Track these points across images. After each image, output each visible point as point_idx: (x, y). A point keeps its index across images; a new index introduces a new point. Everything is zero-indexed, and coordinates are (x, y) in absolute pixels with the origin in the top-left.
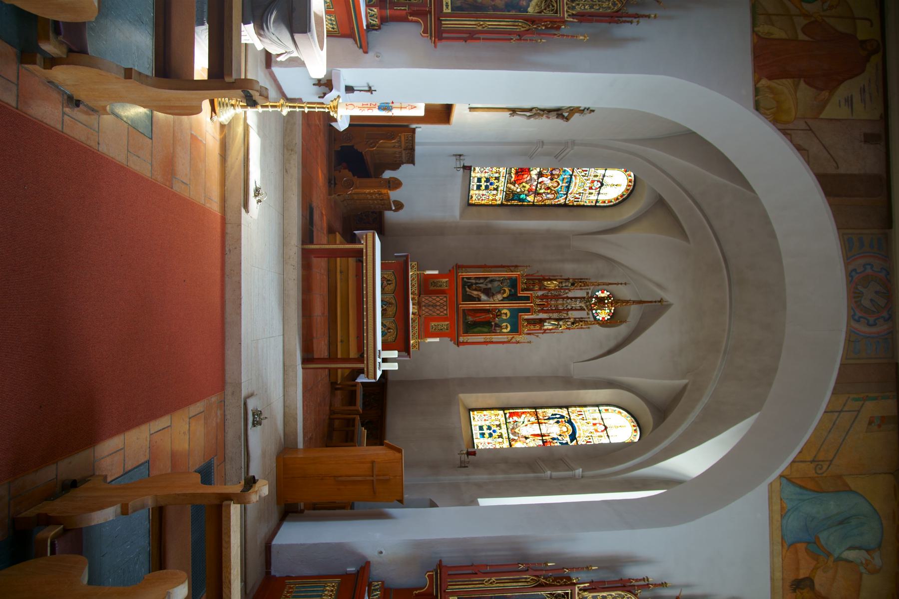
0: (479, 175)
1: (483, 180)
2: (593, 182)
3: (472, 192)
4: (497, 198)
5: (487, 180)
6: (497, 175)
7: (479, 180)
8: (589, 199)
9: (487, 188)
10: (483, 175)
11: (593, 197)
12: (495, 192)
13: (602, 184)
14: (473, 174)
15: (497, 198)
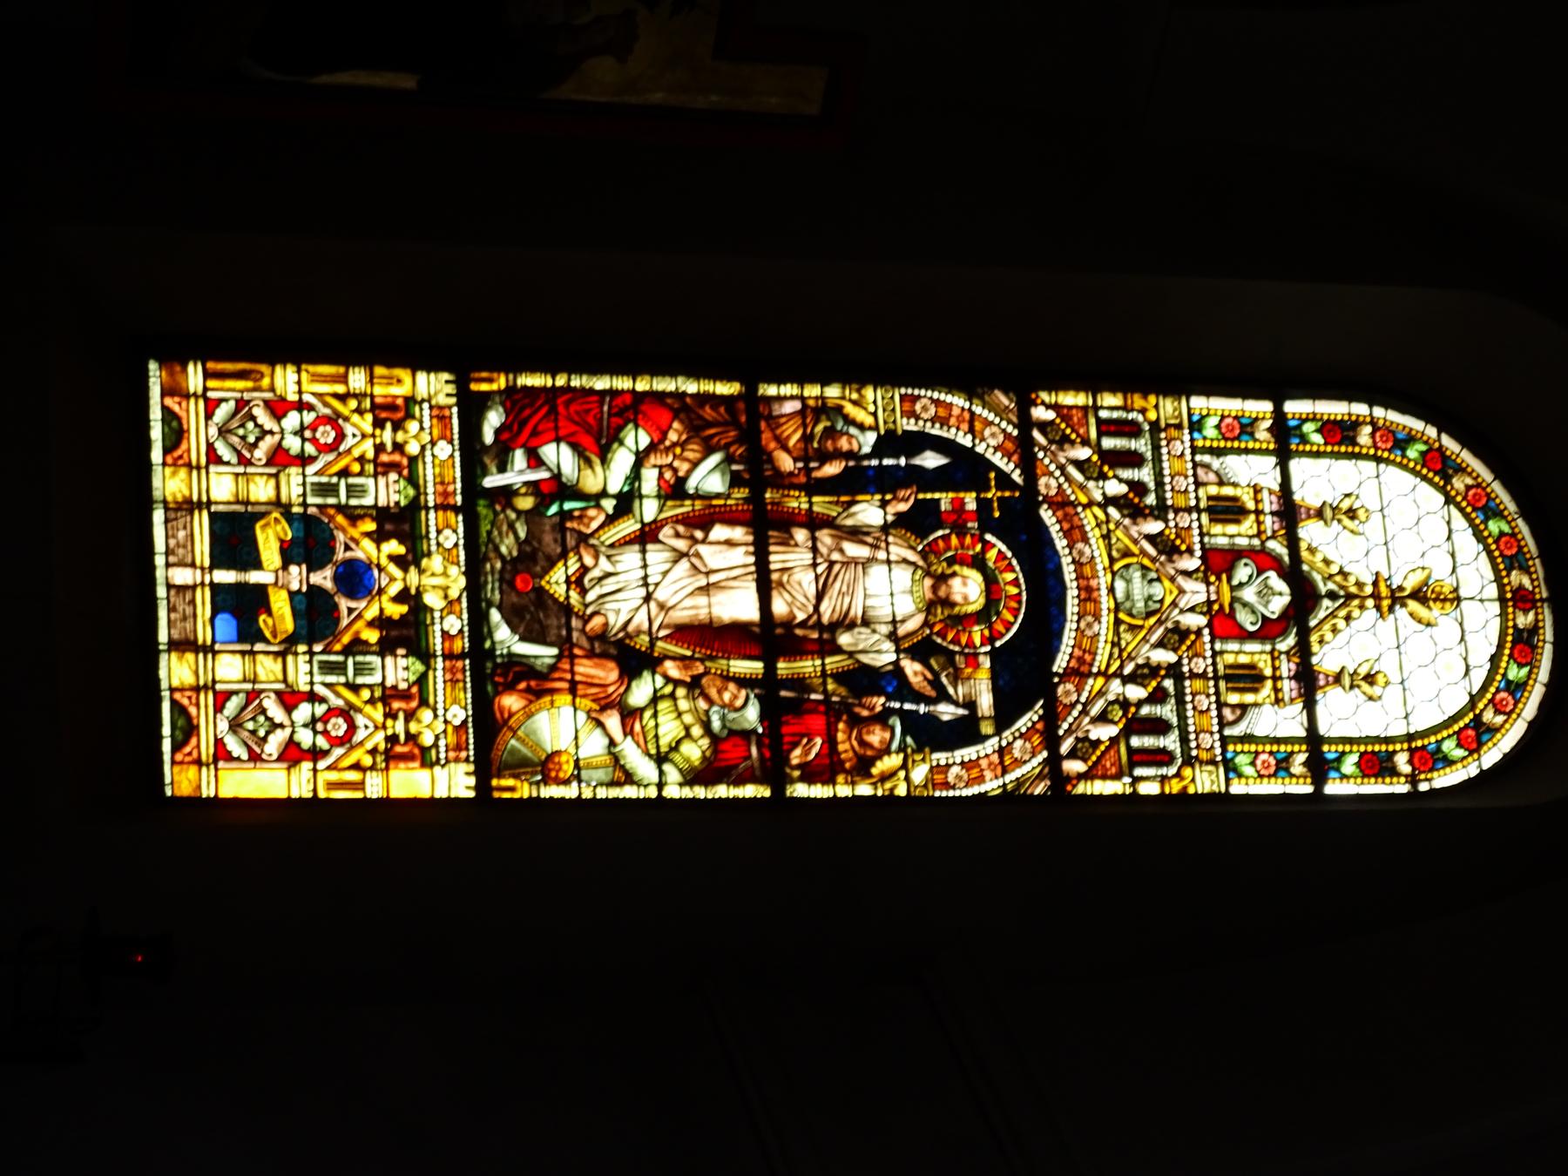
0: (222, 487)
1: (269, 540)
2: (1218, 563)
3: (176, 671)
4: (427, 728)
5: (310, 541)
6: (388, 492)
7: (234, 536)
8: (1251, 749)
9: (316, 618)
10: (261, 491)
11: (1277, 719)
12: (399, 670)
13: (1304, 596)
14: (169, 484)
15: (427, 728)
